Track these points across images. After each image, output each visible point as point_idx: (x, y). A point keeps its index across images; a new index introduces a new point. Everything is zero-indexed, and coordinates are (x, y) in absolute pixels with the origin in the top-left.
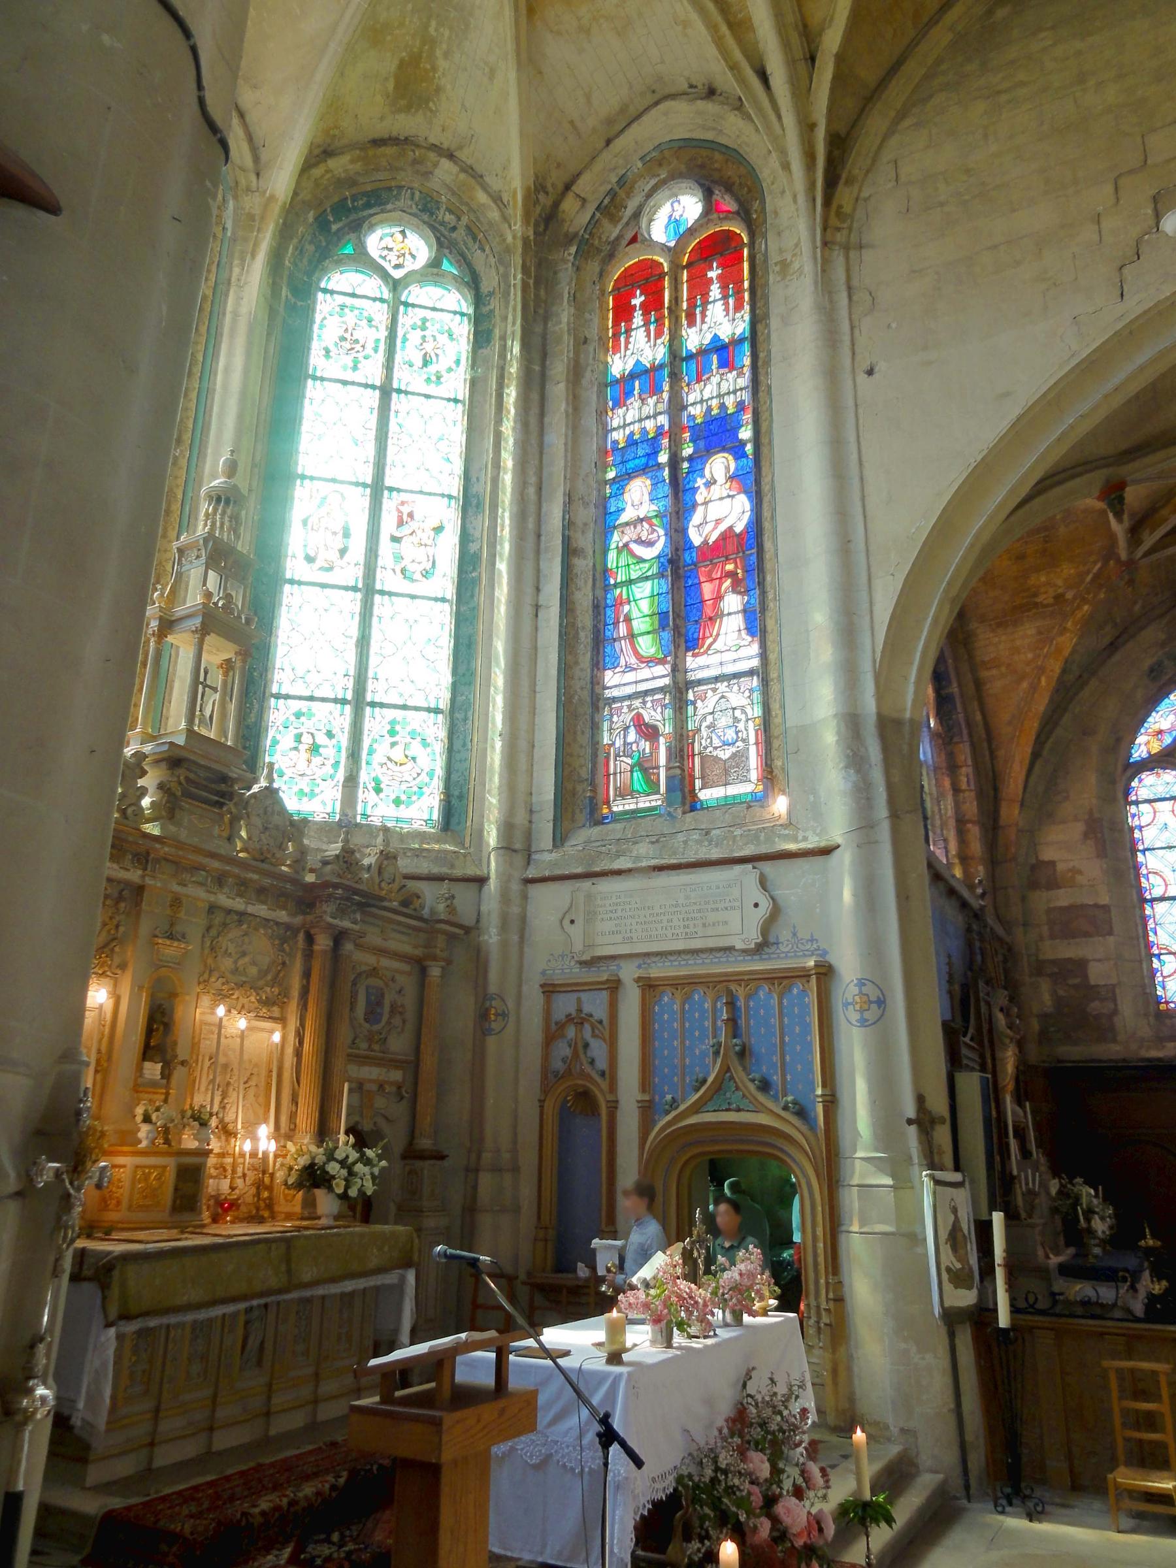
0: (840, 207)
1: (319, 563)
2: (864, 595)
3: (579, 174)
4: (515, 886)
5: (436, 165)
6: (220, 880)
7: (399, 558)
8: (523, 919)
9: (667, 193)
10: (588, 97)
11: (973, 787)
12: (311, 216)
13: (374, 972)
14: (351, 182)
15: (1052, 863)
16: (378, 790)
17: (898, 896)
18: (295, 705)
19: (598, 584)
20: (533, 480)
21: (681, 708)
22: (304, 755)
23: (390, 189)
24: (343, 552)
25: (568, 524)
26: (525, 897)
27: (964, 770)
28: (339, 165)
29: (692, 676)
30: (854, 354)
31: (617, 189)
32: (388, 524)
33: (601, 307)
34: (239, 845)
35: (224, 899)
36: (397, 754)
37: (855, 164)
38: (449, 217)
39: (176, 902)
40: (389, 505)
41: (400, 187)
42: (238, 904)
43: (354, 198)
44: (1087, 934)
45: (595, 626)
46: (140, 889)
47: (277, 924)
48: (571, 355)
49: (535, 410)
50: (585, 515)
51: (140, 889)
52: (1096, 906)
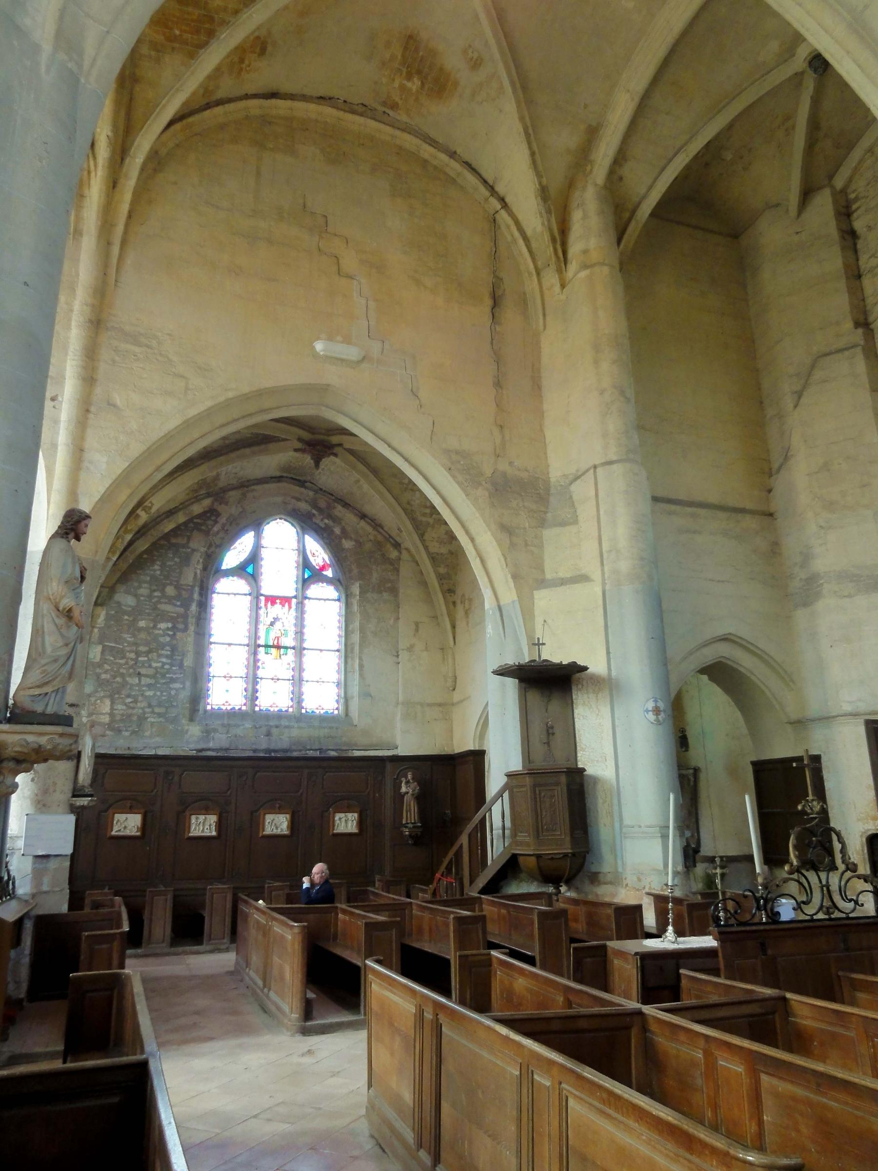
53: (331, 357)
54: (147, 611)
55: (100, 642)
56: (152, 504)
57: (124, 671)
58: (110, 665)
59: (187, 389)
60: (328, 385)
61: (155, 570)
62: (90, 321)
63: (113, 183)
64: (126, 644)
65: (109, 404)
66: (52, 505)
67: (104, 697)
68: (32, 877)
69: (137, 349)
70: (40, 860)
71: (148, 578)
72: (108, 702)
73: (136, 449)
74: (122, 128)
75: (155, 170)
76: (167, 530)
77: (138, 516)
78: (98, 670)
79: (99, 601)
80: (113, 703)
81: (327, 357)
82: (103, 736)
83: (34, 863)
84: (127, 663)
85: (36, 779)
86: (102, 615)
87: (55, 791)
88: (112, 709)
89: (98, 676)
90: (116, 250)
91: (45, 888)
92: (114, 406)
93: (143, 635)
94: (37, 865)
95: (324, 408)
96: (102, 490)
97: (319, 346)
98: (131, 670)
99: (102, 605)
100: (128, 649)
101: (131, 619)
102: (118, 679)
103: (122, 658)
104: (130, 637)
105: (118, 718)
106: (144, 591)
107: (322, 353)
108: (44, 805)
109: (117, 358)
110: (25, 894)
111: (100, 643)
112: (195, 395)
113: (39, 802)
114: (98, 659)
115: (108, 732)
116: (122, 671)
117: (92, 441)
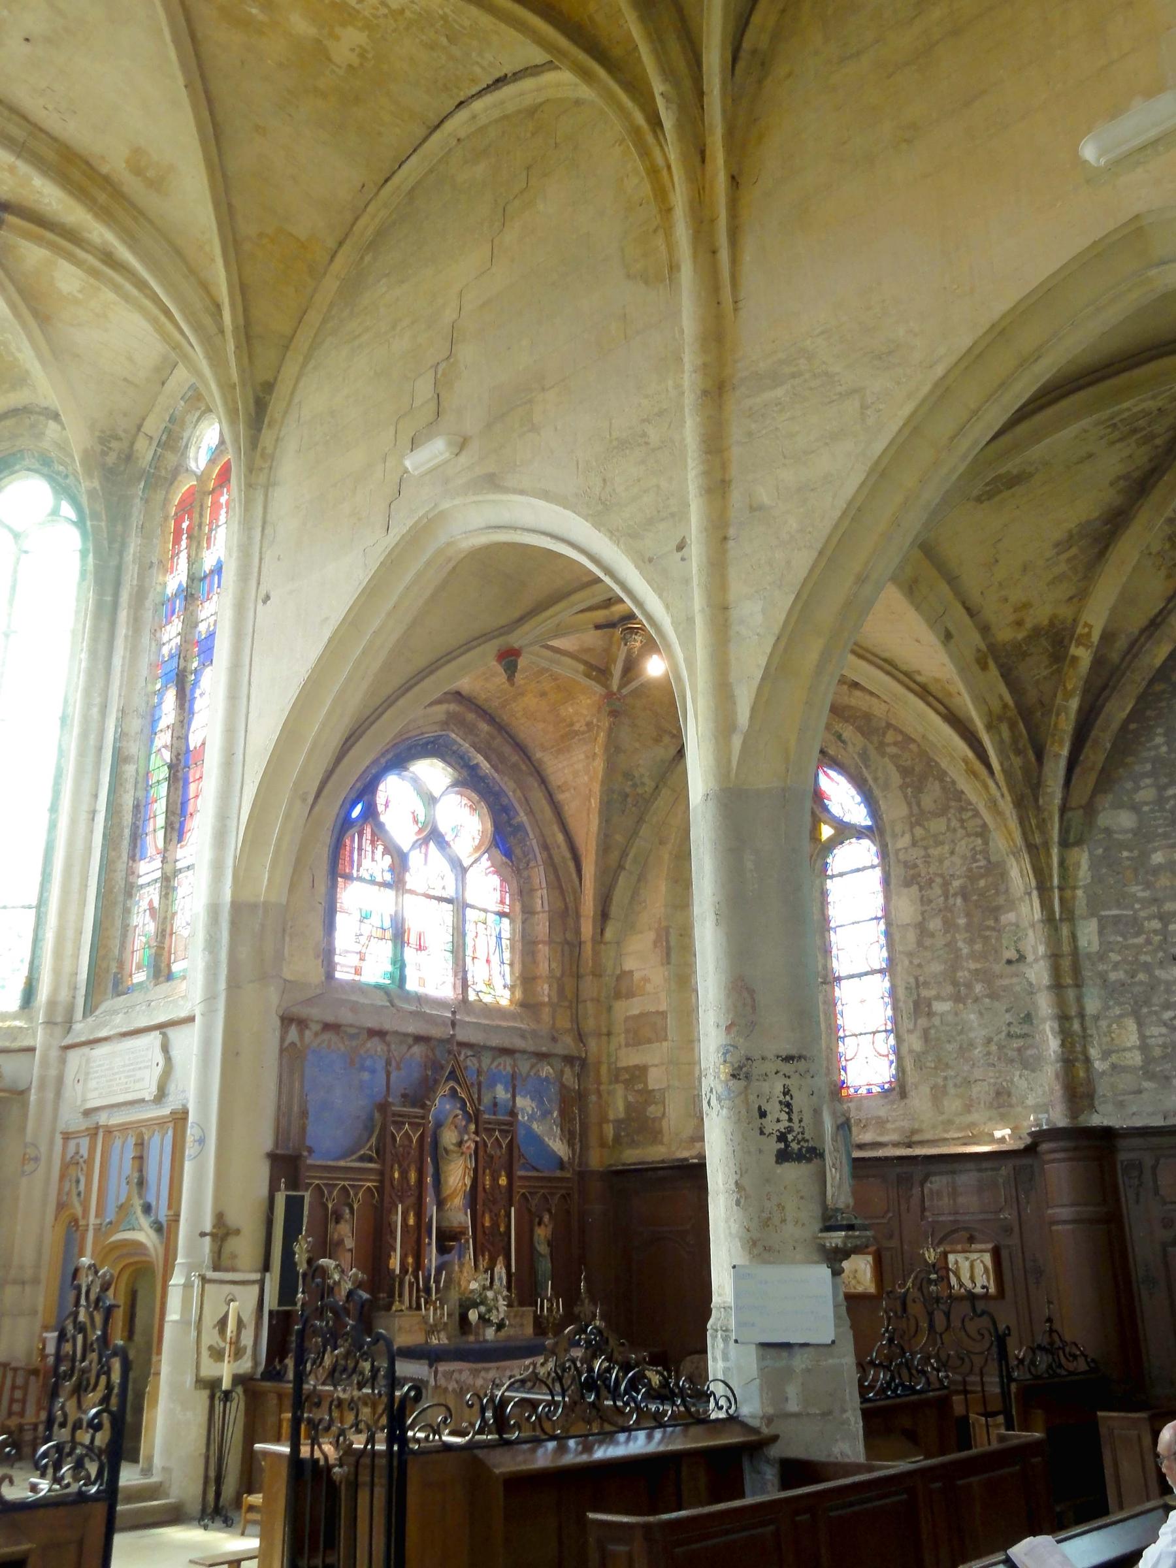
0: (264, 448)
2: (237, 799)
3: (144, 419)
4: (54, 1053)
5: (46, 426)
8: (60, 1080)
9: (206, 422)
10: (130, 359)
11: (546, 908)
15: (631, 972)
19: (139, 786)
20: (97, 700)
21: (167, 894)
23: (14, 454)
25: (121, 736)
26: (63, 1061)
27: (539, 893)
29: (179, 865)
30: (259, 584)
31: (170, 425)
33: (163, 532)
37: (276, 407)
38: (61, 468)
41: (21, 451)
44: (650, 1041)
45: (134, 824)
48: (135, 582)
49: (104, 636)
50: (135, 724)
52: (657, 1012)
53: (1128, 155)
54: (1160, 831)
55: (1093, 914)
56: (1091, 627)
57: (1148, 959)
58: (1119, 952)
59: (864, 407)
60: (1137, 217)
61: (1157, 747)
62: (705, 393)
63: (699, 154)
64: (1137, 906)
65: (752, 509)
66: (700, 719)
67: (1121, 1016)
68: (761, 1386)
69: (779, 392)
70: (772, 1352)
71: (1148, 767)
72: (1131, 1024)
73: (803, 561)
74: (681, 66)
75: (760, 82)
76: (1158, 662)
77: (1075, 659)
78: (1101, 967)
79: (1072, 840)
80: (1140, 1025)
81: (1118, 162)
82: (1139, 1092)
83: (761, 1358)
84: (1148, 942)
85: (742, 1201)
86: (1082, 859)
87: (783, 1221)
88: (1142, 1037)
89: (1103, 977)
90: (724, 255)
91: (793, 1406)
92: (761, 508)
93: (1164, 881)
94: (768, 1362)
95: (1153, 272)
96: (763, 661)
97: (1089, 152)
98: (1161, 954)
99: (1079, 842)
100: (1142, 914)
101: (1136, 853)
102: (1141, 976)
103: (1138, 934)
104: (1143, 890)
105: (1157, 1052)
106: (1146, 794)
107: (1102, 161)
109: (753, 426)
110: (753, 1417)
111: (1092, 915)
112: (880, 410)
113: (754, 1243)
114: (1095, 947)
115: (1146, 1084)
116: (1143, 958)
117: (737, 587)
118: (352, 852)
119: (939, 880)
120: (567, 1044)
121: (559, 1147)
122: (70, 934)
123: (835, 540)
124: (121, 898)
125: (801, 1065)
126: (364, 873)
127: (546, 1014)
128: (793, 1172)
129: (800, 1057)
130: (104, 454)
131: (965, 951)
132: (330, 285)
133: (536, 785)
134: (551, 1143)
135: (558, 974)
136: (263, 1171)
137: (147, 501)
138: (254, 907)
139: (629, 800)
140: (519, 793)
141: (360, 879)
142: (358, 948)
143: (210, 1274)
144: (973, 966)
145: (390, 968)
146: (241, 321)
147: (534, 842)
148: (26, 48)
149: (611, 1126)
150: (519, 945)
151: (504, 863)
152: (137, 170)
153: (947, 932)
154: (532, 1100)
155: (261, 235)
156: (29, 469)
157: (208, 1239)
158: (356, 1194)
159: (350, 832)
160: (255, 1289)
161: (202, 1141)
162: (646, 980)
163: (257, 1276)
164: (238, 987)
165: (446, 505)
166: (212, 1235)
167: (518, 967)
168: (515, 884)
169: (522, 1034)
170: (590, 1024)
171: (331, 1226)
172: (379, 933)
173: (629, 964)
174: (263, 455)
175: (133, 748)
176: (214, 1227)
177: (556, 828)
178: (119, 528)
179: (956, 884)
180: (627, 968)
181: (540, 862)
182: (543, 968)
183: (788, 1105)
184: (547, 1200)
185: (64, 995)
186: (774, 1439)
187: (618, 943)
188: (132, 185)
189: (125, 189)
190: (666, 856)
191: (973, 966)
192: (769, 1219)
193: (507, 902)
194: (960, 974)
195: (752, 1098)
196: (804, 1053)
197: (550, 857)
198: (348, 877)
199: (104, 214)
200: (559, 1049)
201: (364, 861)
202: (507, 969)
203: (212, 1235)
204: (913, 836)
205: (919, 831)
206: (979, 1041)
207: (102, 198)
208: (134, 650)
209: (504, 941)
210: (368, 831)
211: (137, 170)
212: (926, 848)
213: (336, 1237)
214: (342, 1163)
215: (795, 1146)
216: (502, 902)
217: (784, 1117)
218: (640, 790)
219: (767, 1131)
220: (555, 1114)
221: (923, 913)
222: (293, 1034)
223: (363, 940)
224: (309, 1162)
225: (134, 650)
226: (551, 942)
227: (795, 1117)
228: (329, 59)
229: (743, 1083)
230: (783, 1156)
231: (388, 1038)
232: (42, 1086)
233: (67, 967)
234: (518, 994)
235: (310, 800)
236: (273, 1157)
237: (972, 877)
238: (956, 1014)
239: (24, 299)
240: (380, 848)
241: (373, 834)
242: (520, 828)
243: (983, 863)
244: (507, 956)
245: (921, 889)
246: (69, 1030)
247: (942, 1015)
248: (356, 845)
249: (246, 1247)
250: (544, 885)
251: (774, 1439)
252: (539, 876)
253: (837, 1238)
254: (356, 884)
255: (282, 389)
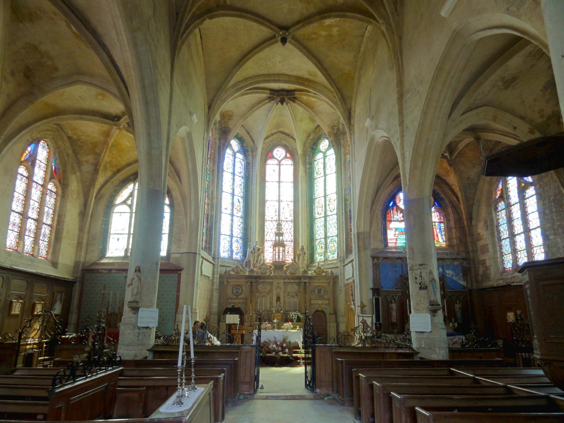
1: (319, 214)
4: (342, 267)
6: (285, 279)
7: (330, 208)
12: (309, 150)
13: (318, 286)
14: (314, 139)
16: (330, 252)
17: (359, 267)
18: (319, 240)
20: (340, 188)
22: (320, 249)
23: (320, 135)
24: (322, 210)
25: (345, 195)
26: (344, 269)
27: (451, 215)
28: (311, 137)
32: (328, 203)
34: (287, 273)
35: (286, 281)
36: (332, 245)
39: (278, 283)
40: (327, 199)
42: (289, 281)
43: (316, 141)
44: (486, 253)
46: (272, 282)
47: (297, 282)
51: (272, 282)
62: (398, 99)
70: (419, 333)
91: (423, 346)
108: (418, 310)
118: (391, 215)
119: (547, 197)
120: (464, 255)
121: (463, 283)
122: (342, 241)
123: (419, 133)
124: (349, 232)
125: (424, 266)
126: (394, 219)
127: (456, 248)
128: (423, 292)
129: (423, 264)
130: (333, 131)
131: (556, 219)
132: (356, 81)
133: (445, 186)
134: (460, 282)
135: (459, 236)
136: (371, 293)
137: (343, 139)
138: (362, 233)
139: (471, 185)
140: (440, 189)
141: (394, 221)
142: (395, 238)
143: (360, 315)
144: (558, 223)
145: (405, 241)
146: (340, 97)
147: (447, 202)
148: (281, 64)
149: (480, 277)
150: (446, 230)
151: (440, 209)
152: (310, 75)
153: (551, 213)
154: (452, 271)
155: (338, 76)
156: (324, 138)
157: (360, 307)
158: (396, 297)
159: (390, 209)
160: (371, 318)
161: (357, 286)
162: (483, 235)
163: (371, 316)
164: (360, 252)
165: (373, 134)
166: (360, 306)
167: (447, 235)
168: (444, 214)
169: (447, 254)
170: (470, 249)
171: (390, 304)
172: (401, 233)
173: (479, 231)
174: (352, 126)
175: (348, 197)
176: (360, 304)
177: (453, 196)
178: (339, 147)
179: (552, 198)
180: (479, 232)
181: (449, 206)
182: (454, 235)
183: (421, 276)
184: (458, 297)
185: (342, 255)
186: (419, 353)
187: (476, 225)
188: (311, 78)
189: (311, 79)
190: (484, 199)
191: (558, 223)
192: (418, 303)
193: (442, 218)
194: (555, 226)
195: (414, 275)
196: (425, 263)
197: (453, 205)
198: (391, 221)
199: (308, 86)
200: (460, 257)
201: (395, 216)
202: (444, 237)
203: (360, 306)
204: (540, 185)
205: (541, 183)
206: (561, 247)
207: (307, 83)
208: (345, 175)
209: (442, 230)
210: (395, 208)
211: (310, 75)
212: (543, 188)
213: (391, 307)
214: (391, 290)
215: (423, 286)
216: (440, 219)
217: (420, 279)
218: (474, 182)
219: (417, 282)
220: (461, 274)
221: (544, 208)
222: (376, 260)
223: (396, 235)
224: (382, 290)
225: (345, 175)
226: (455, 228)
227: (422, 279)
228: (333, 36)
229: (411, 271)
230: (421, 288)
231: (403, 259)
232: (341, 274)
233: (342, 249)
234: (448, 243)
235: (370, 206)
236: (372, 289)
237: (555, 195)
238: (555, 239)
239: (307, 106)
240: (399, 212)
241: (396, 209)
242: (442, 199)
243: (557, 191)
244: (443, 233)
245: (543, 201)
246: (344, 262)
247: (551, 239)
248: (392, 212)
249: (368, 309)
250: (451, 212)
251: (419, 353)
252: (450, 210)
253: (434, 308)
254: (393, 222)
255: (353, 109)
